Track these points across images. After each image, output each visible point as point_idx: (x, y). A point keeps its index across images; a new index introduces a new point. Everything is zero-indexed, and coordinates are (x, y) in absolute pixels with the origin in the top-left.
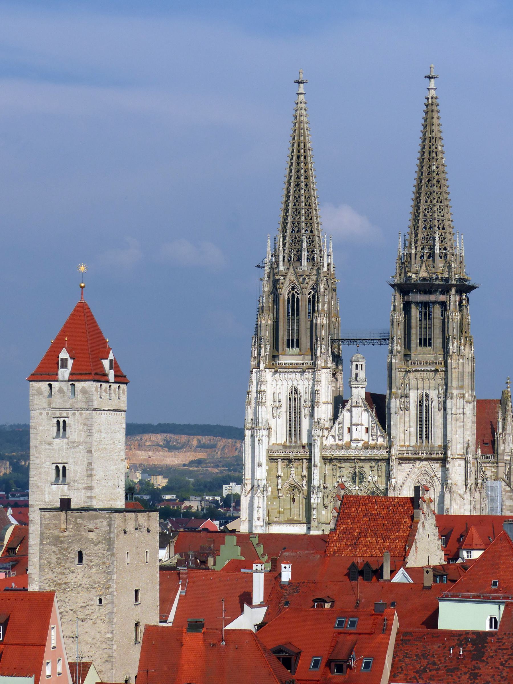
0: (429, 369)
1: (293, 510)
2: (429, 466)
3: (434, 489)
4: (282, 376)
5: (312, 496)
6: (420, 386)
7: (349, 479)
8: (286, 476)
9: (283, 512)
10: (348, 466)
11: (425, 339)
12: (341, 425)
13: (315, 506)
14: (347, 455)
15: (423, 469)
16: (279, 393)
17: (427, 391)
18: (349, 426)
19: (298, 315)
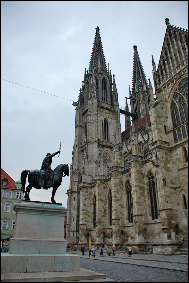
11: (104, 98)
17: (107, 118)
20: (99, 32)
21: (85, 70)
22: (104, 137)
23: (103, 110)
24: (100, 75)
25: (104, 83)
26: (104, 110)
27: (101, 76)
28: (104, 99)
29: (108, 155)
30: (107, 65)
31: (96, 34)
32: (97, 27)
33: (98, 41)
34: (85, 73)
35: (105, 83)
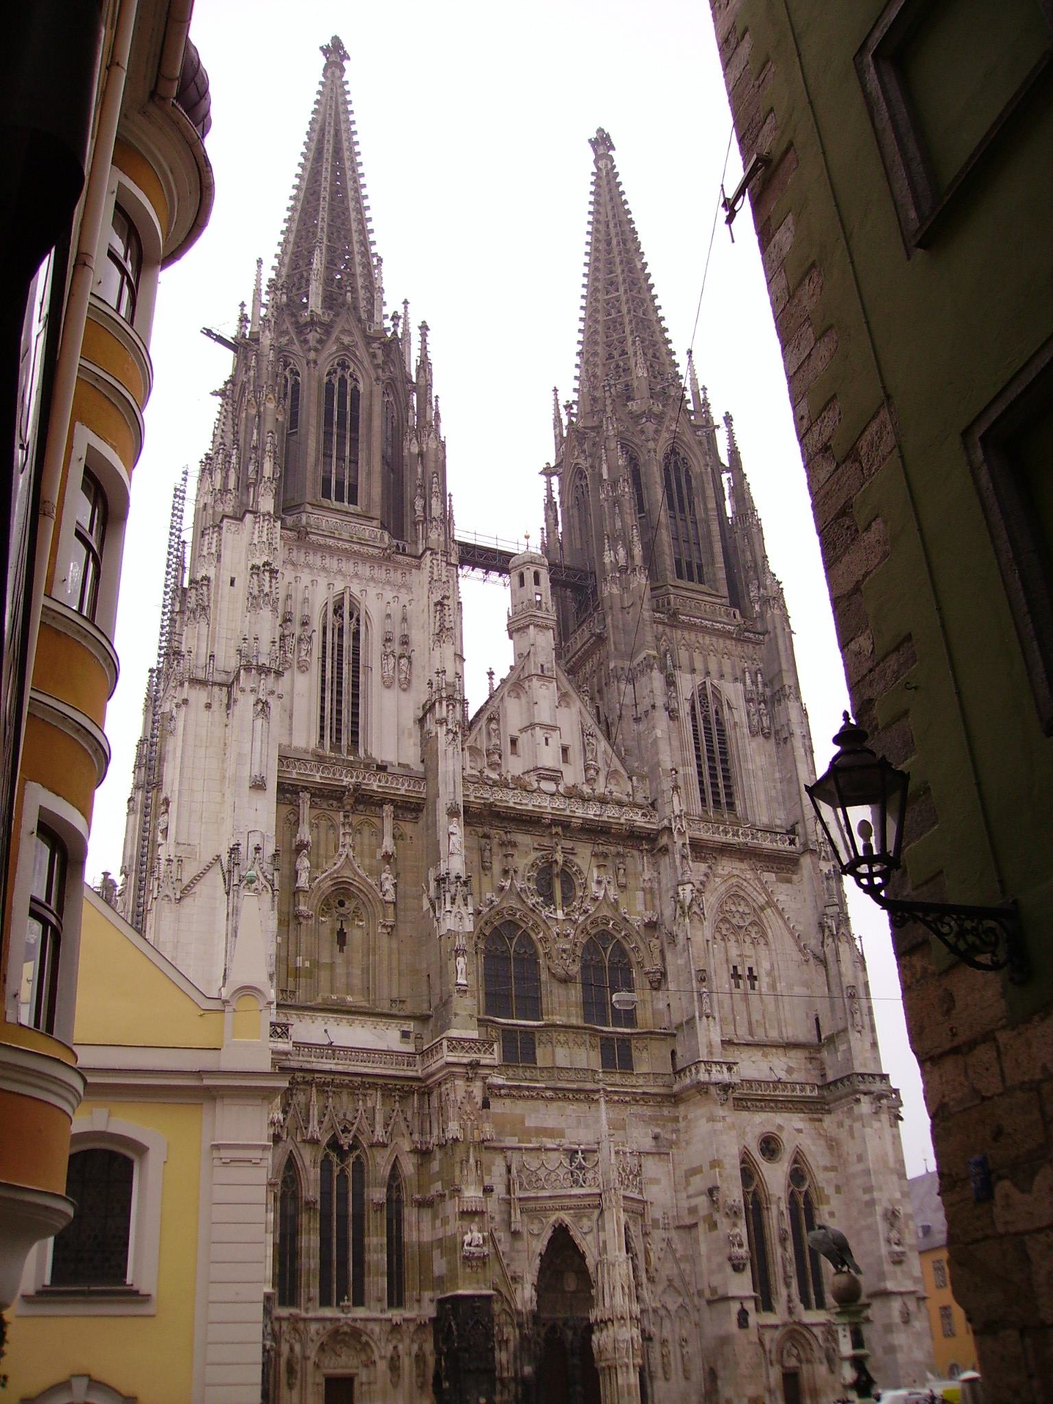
0: (719, 626)
1: (340, 971)
2: (749, 875)
3: (767, 944)
4: (315, 559)
5: (448, 907)
6: (699, 665)
7: (533, 886)
8: (322, 852)
9: (310, 973)
10: (527, 845)
12: (493, 726)
13: (461, 942)
14: (531, 808)
15: (734, 880)
16: (306, 600)
17: (715, 682)
18: (517, 734)
19: (355, 428)
20: (612, 161)
21: (556, 400)
22: (709, 790)
23: (687, 636)
24: (650, 427)
25: (677, 469)
26: (693, 638)
27: (657, 431)
28: (690, 570)
29: (743, 898)
30: (680, 358)
31: (593, 174)
32: (600, 130)
33: (614, 215)
34: (558, 420)
35: (683, 470)
